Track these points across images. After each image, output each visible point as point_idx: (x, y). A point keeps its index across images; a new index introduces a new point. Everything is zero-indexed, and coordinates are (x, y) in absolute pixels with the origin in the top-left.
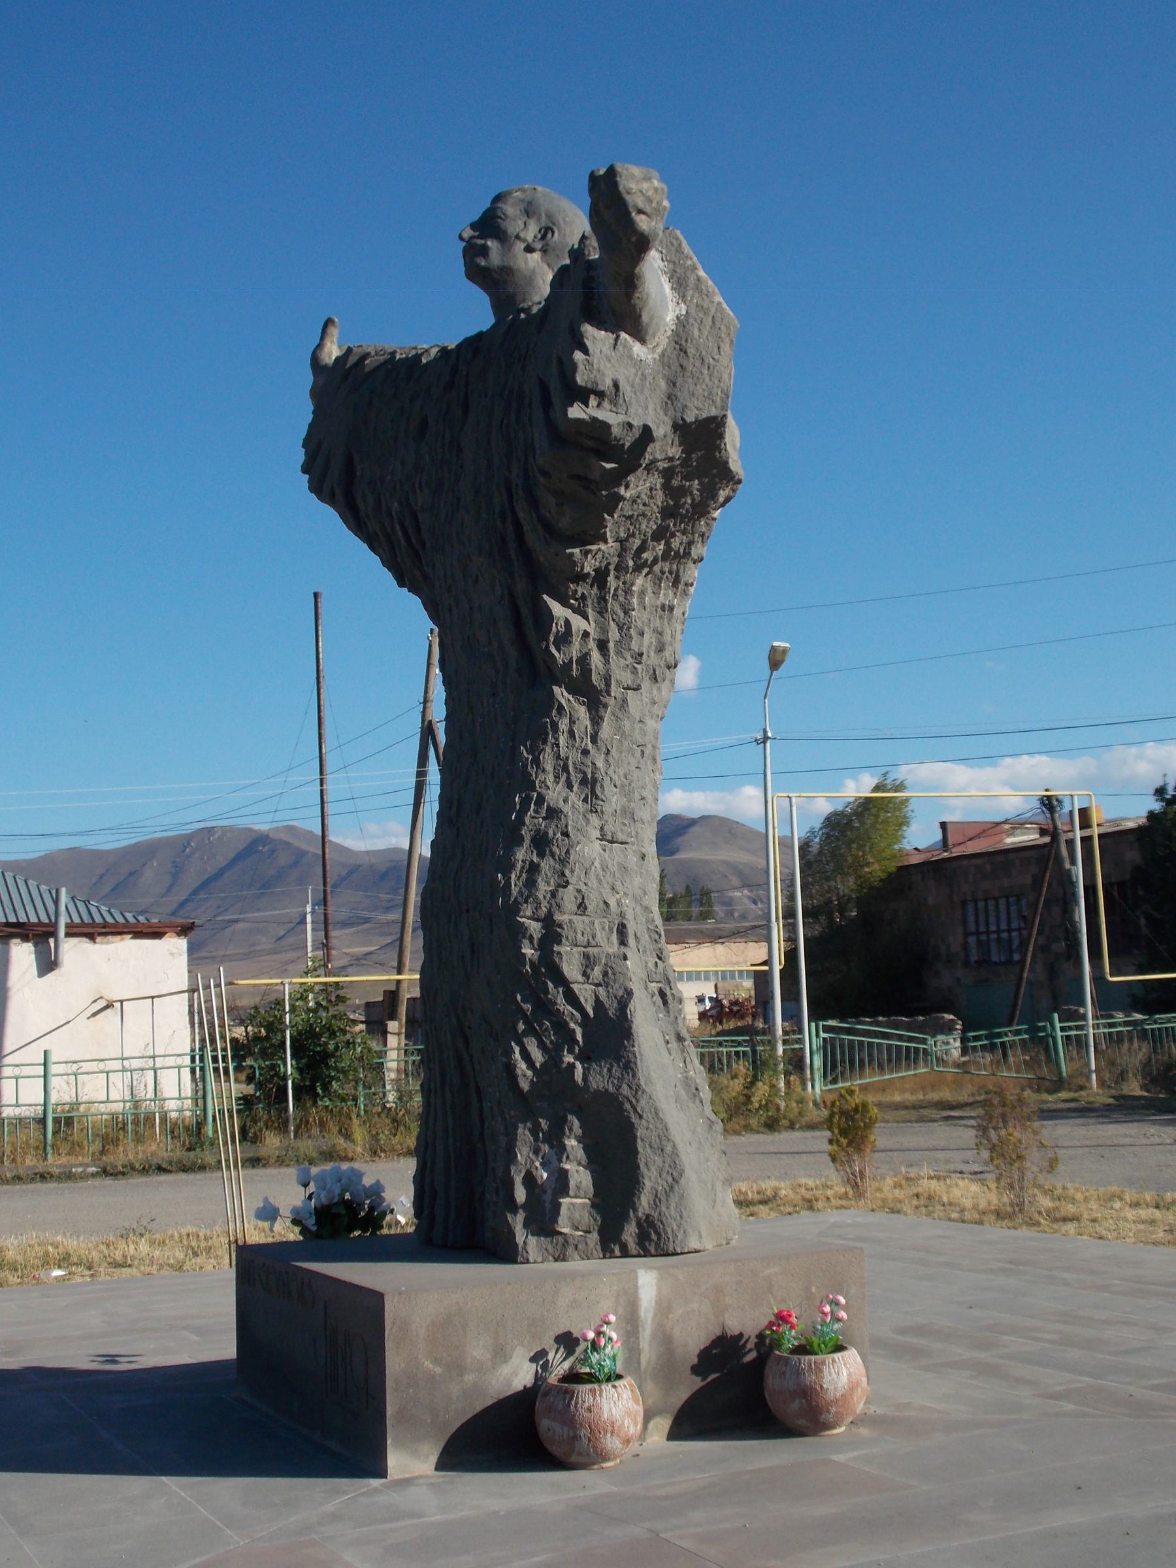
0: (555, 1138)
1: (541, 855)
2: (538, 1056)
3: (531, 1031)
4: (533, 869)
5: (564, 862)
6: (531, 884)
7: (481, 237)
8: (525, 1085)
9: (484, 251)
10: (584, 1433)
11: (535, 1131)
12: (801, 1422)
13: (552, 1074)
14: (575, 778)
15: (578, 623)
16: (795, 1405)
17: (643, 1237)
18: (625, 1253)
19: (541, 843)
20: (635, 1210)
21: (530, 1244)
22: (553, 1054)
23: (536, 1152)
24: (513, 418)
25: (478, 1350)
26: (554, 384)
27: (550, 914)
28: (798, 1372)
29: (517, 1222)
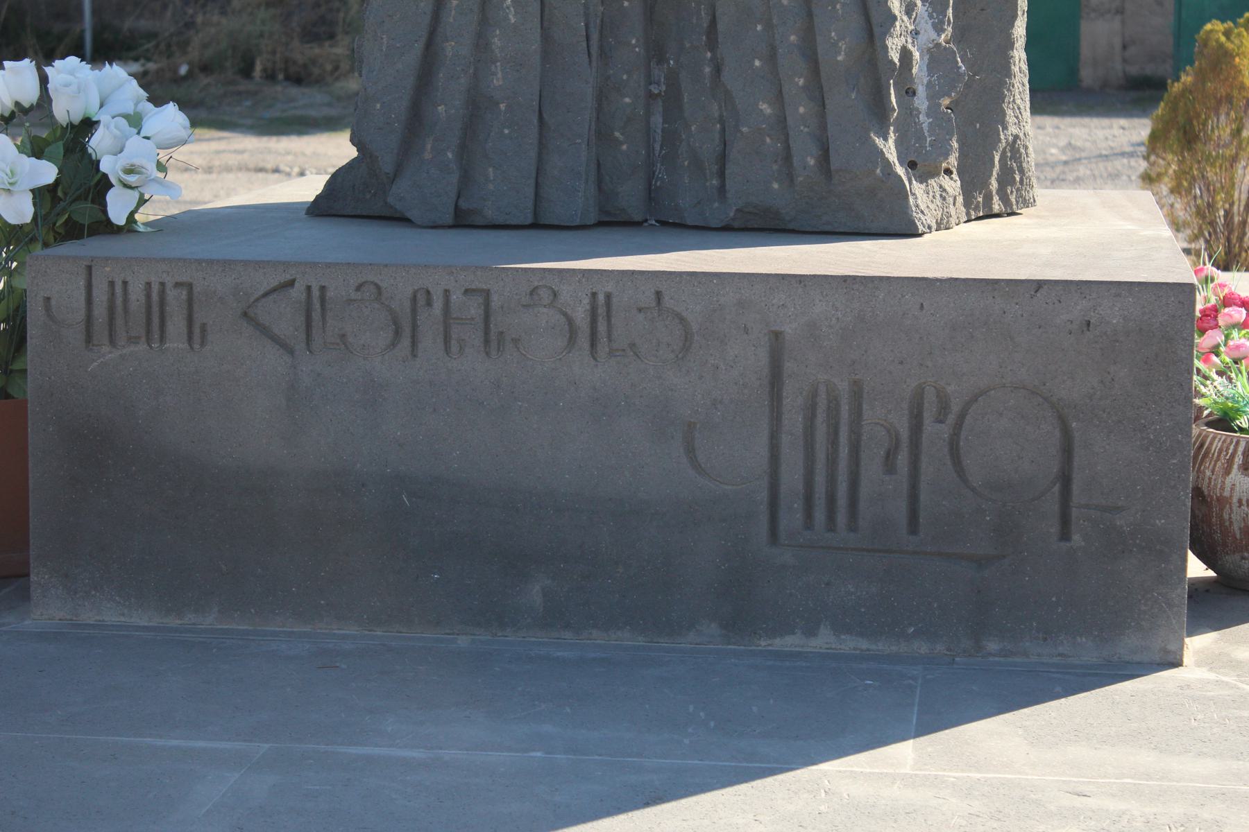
17: (1006, 179)
20: (1005, 128)
21: (922, 198)
29: (889, 148)
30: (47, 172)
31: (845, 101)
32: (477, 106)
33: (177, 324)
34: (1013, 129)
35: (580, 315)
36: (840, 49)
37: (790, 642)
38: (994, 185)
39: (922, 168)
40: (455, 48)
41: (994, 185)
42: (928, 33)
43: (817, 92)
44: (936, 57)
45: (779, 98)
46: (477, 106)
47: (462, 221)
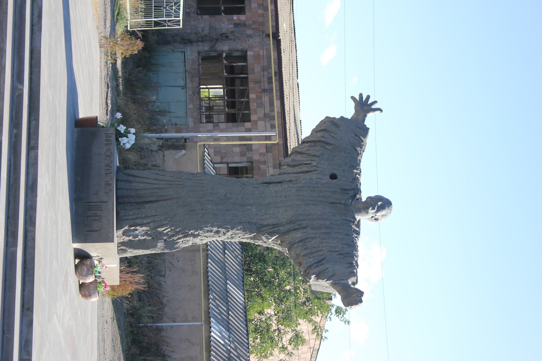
0: (146, 234)
1: (215, 232)
2: (165, 232)
3: (172, 230)
4: (211, 231)
5: (213, 237)
6: (208, 231)
7: (378, 206)
8: (159, 229)
9: (373, 209)
10: (84, 278)
11: (147, 230)
12: (83, 293)
13: (161, 233)
14: (233, 236)
15: (270, 240)
16: (87, 293)
17: (122, 250)
18: (118, 247)
19: (218, 232)
21: (121, 232)
22: (167, 234)
23: (143, 231)
24: (323, 231)
25: (100, 251)
26: (321, 268)
27: (200, 236)
28: (94, 293)
29: (126, 228)
30: (122, 132)
31: (132, 222)
32: (131, 182)
33: (107, 142)
34: (129, 250)
35: (109, 183)
36: (138, 221)
37: (74, 205)
38: (122, 247)
39: (124, 233)
40: (137, 179)
41: (122, 247)
42: (140, 234)
43: (133, 219)
44: (137, 236)
45: (132, 215)
46: (131, 182)
47: (117, 181)
